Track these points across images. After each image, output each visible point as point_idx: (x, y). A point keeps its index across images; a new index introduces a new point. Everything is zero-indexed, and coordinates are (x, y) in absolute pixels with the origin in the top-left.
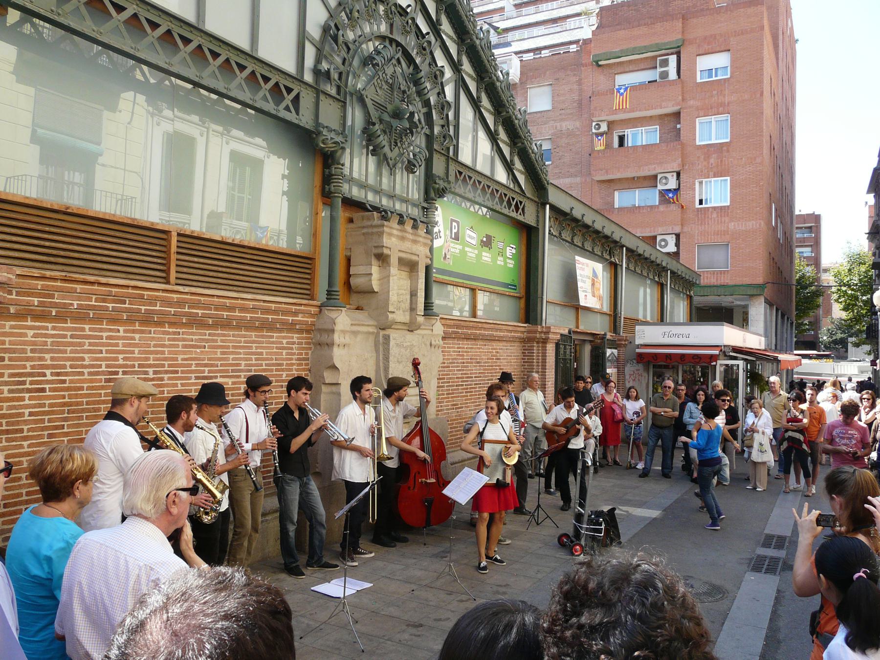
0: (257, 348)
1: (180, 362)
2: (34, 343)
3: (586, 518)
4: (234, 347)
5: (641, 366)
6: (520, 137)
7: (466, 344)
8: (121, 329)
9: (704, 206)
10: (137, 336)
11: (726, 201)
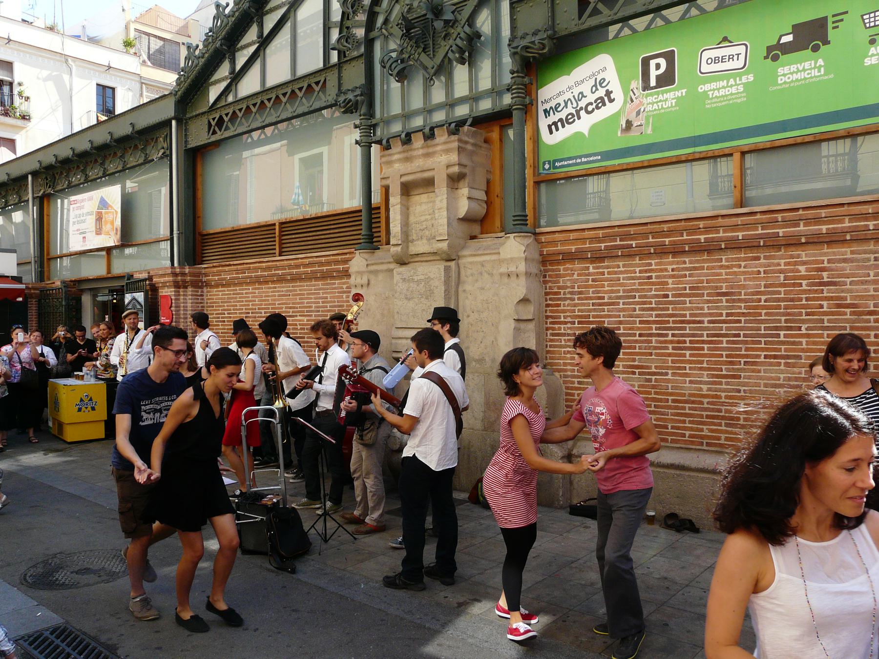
0: (323, 293)
4: (308, 294)
7: (670, 264)
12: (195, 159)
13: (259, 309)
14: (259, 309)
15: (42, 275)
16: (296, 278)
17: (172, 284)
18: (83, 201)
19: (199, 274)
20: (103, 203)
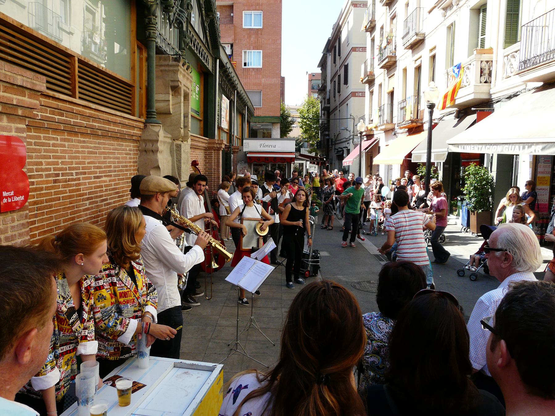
1: (86, 165)
3: (311, 256)
5: (247, 165)
6: (212, 11)
9: (247, 67)
10: (66, 144)
11: (260, 65)
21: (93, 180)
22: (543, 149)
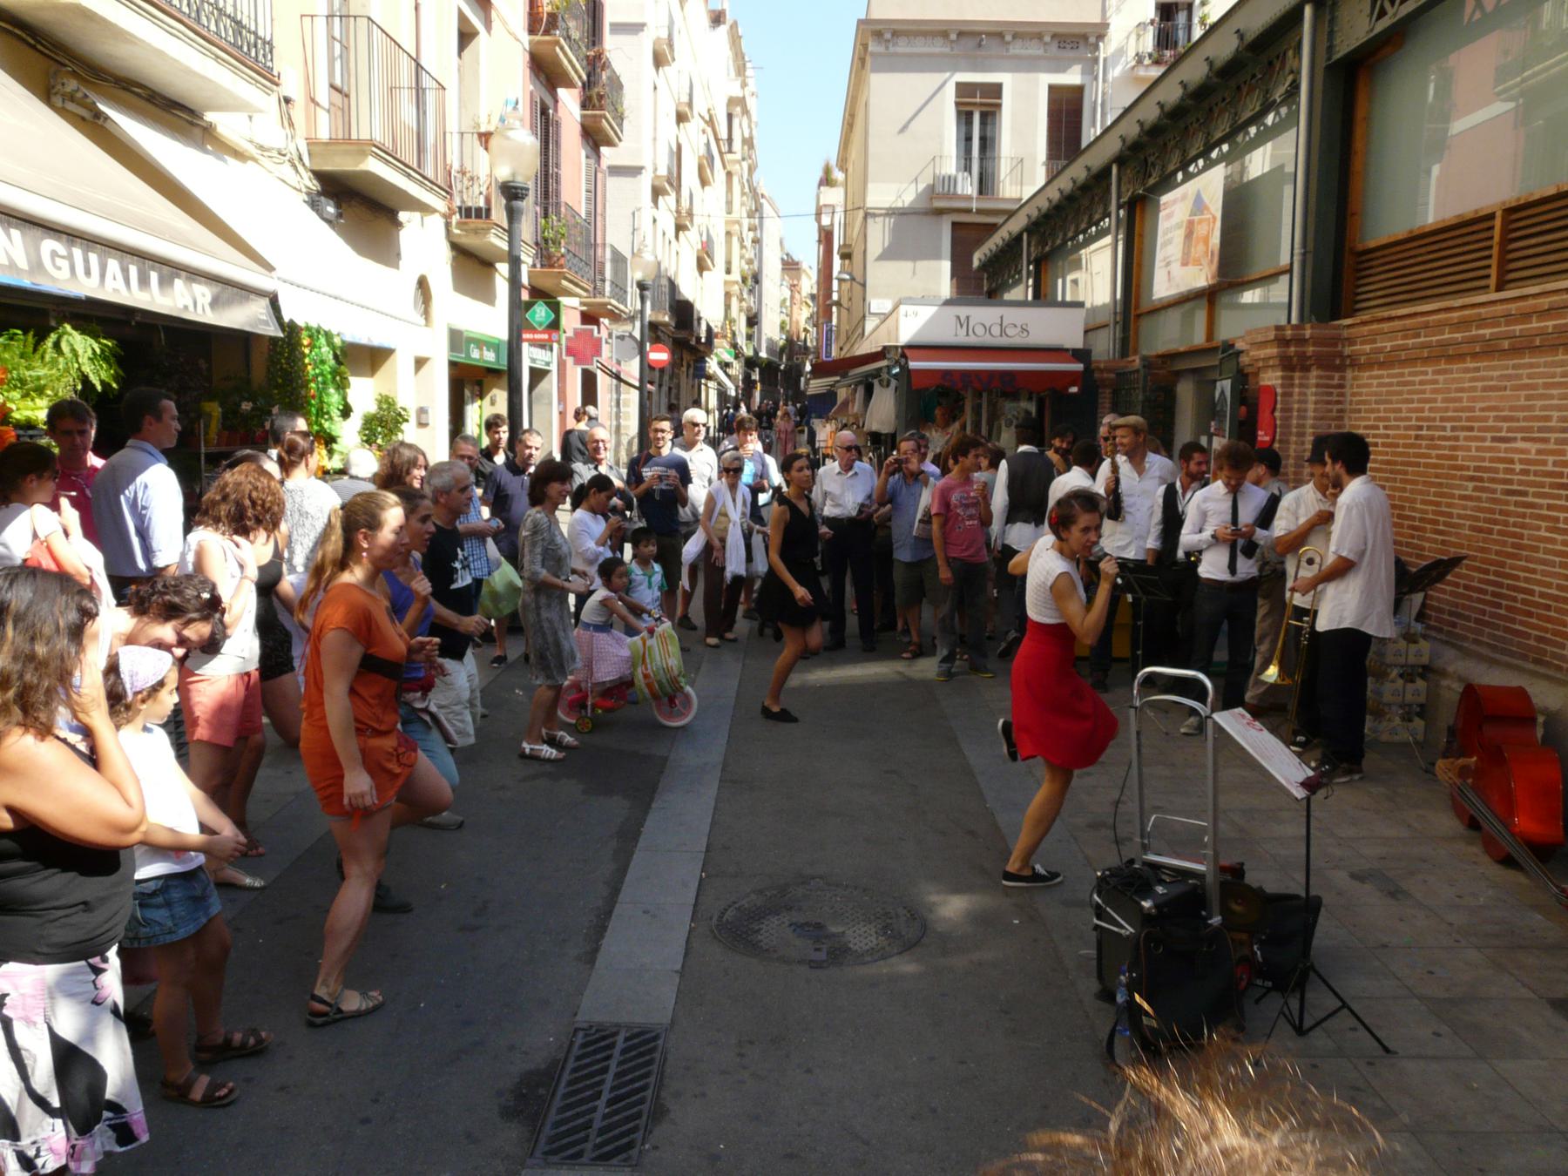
2: (1376, 394)
4: (1547, 386)
8: (1430, 370)
10: (1441, 378)
12: (1351, 84)
13: (1442, 419)
14: (1442, 419)
15: (1126, 345)
16: (1523, 346)
17: (1277, 362)
18: (1175, 202)
19: (1335, 341)
20: (1199, 205)
21: (1488, 444)
22: (215, 303)
